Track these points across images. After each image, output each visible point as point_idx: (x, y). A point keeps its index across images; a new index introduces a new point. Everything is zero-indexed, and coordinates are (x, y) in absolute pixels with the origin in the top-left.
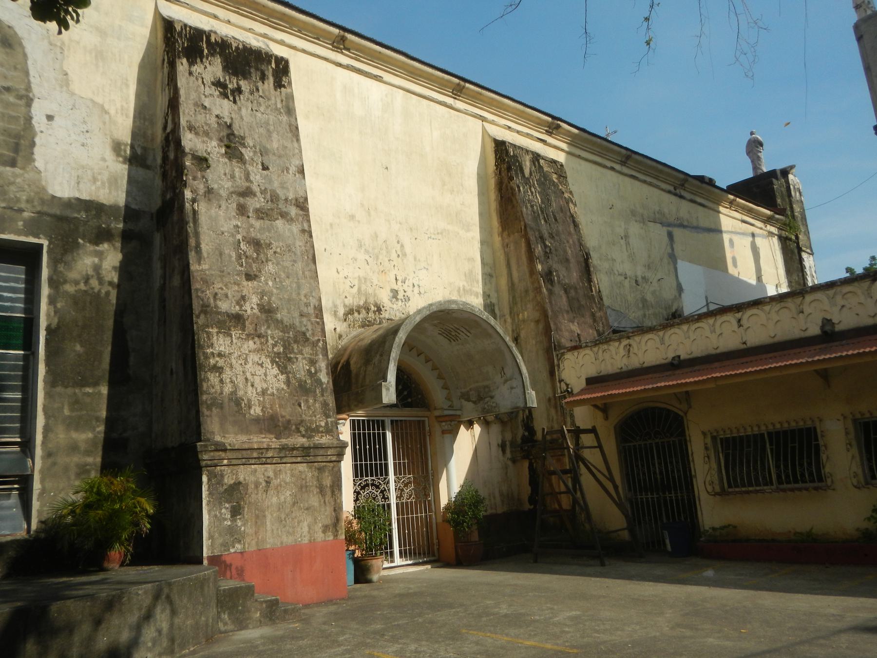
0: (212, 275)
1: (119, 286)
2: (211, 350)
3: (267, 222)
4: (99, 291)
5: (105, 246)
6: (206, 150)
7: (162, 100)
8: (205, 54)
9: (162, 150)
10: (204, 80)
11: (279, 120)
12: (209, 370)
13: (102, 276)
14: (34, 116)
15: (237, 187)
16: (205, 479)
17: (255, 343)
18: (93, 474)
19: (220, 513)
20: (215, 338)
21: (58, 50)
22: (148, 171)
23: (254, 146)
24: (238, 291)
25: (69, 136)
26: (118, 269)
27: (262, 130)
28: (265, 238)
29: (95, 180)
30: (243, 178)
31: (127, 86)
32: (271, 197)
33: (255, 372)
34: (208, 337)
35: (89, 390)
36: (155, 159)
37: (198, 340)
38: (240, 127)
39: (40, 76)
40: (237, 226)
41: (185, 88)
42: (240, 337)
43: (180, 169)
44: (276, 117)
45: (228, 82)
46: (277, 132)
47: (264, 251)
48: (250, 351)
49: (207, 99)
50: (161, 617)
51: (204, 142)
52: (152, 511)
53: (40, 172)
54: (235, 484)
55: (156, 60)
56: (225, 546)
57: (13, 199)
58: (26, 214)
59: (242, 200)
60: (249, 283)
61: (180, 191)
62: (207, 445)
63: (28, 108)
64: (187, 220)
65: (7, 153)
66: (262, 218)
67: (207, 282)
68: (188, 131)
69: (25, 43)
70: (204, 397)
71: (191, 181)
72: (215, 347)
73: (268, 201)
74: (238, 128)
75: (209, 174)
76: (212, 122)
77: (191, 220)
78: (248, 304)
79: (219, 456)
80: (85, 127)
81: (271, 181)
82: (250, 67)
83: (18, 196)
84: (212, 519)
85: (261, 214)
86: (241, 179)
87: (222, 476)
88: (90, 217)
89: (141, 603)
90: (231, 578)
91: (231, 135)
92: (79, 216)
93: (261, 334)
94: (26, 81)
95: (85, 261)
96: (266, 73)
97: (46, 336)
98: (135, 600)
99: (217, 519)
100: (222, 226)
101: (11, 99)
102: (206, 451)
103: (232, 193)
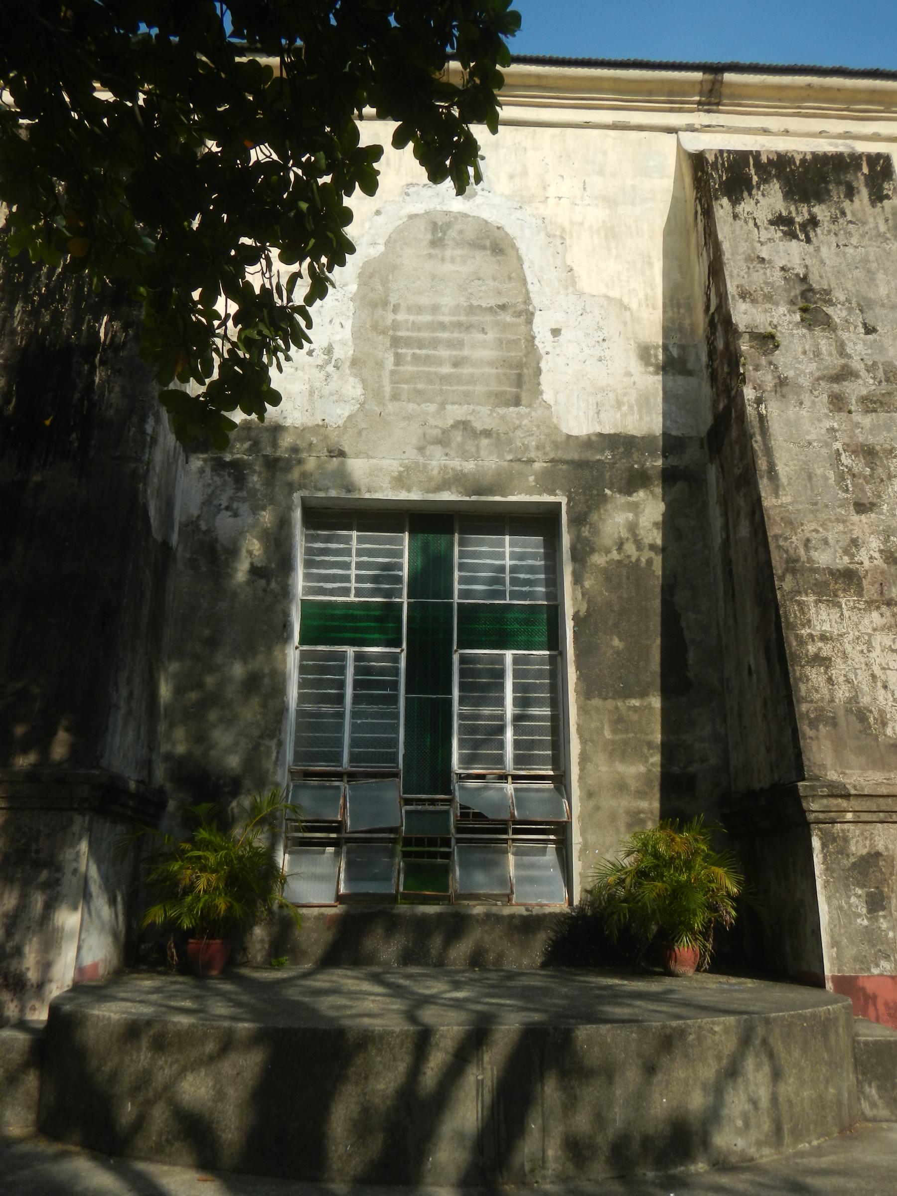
0: (799, 510)
1: (664, 549)
2: (809, 631)
3: (883, 415)
4: (638, 560)
5: (641, 495)
6: (771, 322)
7: (700, 270)
8: (754, 183)
9: (706, 342)
10: (757, 220)
11: (885, 250)
12: (808, 662)
13: (639, 538)
14: (536, 335)
15: (827, 368)
16: (816, 843)
17: (882, 615)
18: (650, 826)
19: (847, 903)
20: (813, 610)
21: (559, 242)
22: (690, 378)
23: (848, 300)
24: (845, 533)
25: (582, 350)
26: (661, 526)
27: (856, 273)
28: (882, 441)
29: (619, 404)
30: (834, 352)
31: (650, 264)
32: (885, 374)
33: (888, 664)
34: (802, 611)
35: (636, 702)
36: (698, 359)
37: (786, 617)
38: (821, 277)
39: (539, 281)
40: (832, 430)
41: (730, 239)
42: (855, 607)
43: (733, 358)
44: (879, 247)
45: (794, 215)
46: (884, 269)
47: (882, 462)
48: (875, 630)
49: (764, 247)
50: (755, 1077)
51: (766, 311)
52: (736, 890)
53: (549, 407)
54: (869, 854)
55: (686, 218)
56: (862, 962)
57: (521, 447)
58: (537, 466)
59: (836, 387)
60: (863, 517)
61: (737, 391)
62: (814, 785)
63: (529, 326)
64: (752, 431)
65: (509, 389)
66: (875, 411)
67: (791, 523)
68: (741, 300)
69: (518, 243)
70: (804, 707)
71: (752, 373)
72: (815, 626)
73: (880, 382)
74: (819, 278)
75: (779, 357)
76: (775, 279)
77: (757, 431)
78: (863, 551)
79: (837, 805)
80: (600, 334)
81: (882, 349)
82: (827, 183)
83: (526, 443)
84: (834, 912)
85: (871, 404)
86: (831, 355)
87: (846, 840)
88: (617, 457)
89: (720, 1047)
90: (877, 1020)
91: (808, 292)
92: (603, 458)
93: (892, 599)
94: (524, 291)
95: (616, 520)
96: (855, 184)
97: (574, 627)
98: (709, 1041)
99: (844, 914)
100: (808, 433)
101: (509, 319)
102: (813, 796)
103: (819, 379)
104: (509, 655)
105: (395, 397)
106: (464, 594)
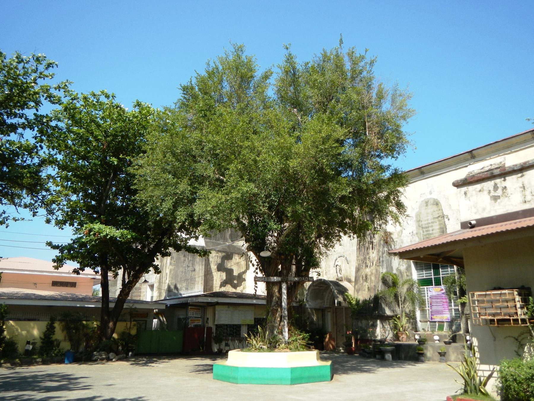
106: (442, 274)
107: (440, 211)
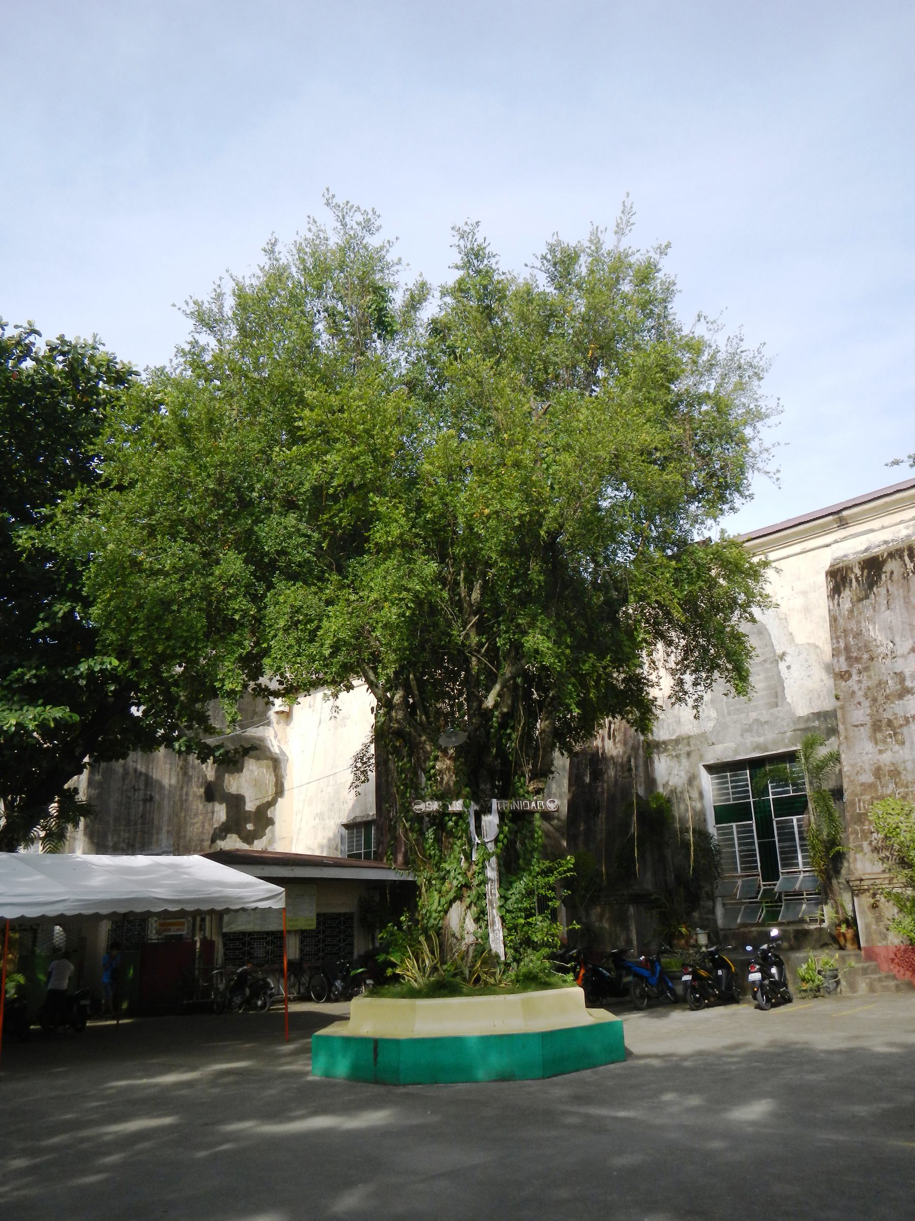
21: (784, 621)
29: (819, 696)
58: (789, 734)
104: (795, 818)
105: (729, 714)
107: (767, 649)
